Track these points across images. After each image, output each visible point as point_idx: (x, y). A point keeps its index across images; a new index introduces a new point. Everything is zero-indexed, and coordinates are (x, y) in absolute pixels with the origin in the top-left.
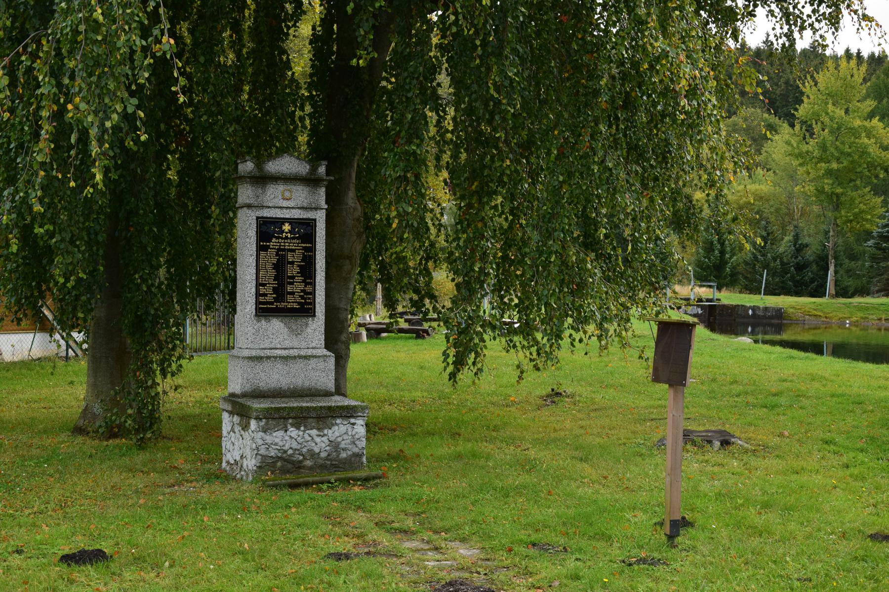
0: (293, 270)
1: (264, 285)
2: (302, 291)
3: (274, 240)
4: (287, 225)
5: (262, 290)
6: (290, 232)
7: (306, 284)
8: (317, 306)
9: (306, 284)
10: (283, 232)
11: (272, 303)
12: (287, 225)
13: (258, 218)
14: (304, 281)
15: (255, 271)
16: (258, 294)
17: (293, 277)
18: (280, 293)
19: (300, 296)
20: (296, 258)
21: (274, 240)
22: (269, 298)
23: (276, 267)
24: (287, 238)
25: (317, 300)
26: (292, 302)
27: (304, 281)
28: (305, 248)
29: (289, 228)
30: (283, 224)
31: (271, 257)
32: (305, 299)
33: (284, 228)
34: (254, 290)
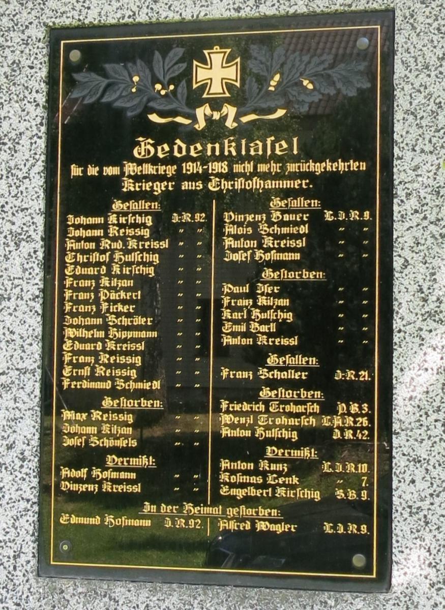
0: (253, 316)
3: (144, 147)
5: (76, 427)
7: (334, 395)
8: (401, 526)
9: (334, 395)
10: (195, 98)
12: (217, 57)
13: (56, 35)
14: (317, 379)
15: (35, 324)
17: (255, 356)
18: (180, 465)
20: (268, 241)
21: (144, 147)
22: (113, 476)
23: (150, 295)
24: (215, 131)
25: (403, 494)
27: (317, 379)
28: (329, 189)
29: (232, 73)
30: (196, 52)
31: (127, 242)
33: (201, 74)
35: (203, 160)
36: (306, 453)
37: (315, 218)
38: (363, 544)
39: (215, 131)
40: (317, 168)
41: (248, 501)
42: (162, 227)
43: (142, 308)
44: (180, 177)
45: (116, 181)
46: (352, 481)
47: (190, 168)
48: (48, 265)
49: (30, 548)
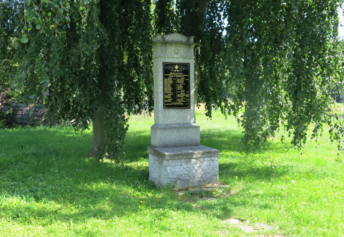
0: (180, 87)
1: (167, 94)
2: (185, 97)
3: (171, 73)
4: (177, 66)
5: (166, 97)
6: (178, 69)
7: (186, 93)
9: (186, 93)
10: (175, 69)
11: (170, 103)
12: (177, 66)
13: (163, 63)
14: (185, 92)
15: (162, 88)
16: (164, 99)
17: (180, 90)
18: (174, 98)
19: (183, 99)
20: (181, 81)
21: (171, 73)
22: (169, 100)
23: (172, 85)
25: (191, 101)
26: (180, 102)
27: (185, 92)
28: (185, 77)
29: (178, 67)
30: (175, 65)
31: (170, 81)
32: (186, 101)
33: (175, 67)
34: (162, 97)
35: (176, 74)
36: (184, 98)
37: (184, 79)
38: (188, 105)
39: (177, 72)
40: (185, 75)
41: (180, 102)
42: (173, 80)
43: (171, 87)
44: (174, 76)
45: (169, 76)
46: (188, 100)
47: (175, 75)
48: (163, 83)
49: (163, 107)
